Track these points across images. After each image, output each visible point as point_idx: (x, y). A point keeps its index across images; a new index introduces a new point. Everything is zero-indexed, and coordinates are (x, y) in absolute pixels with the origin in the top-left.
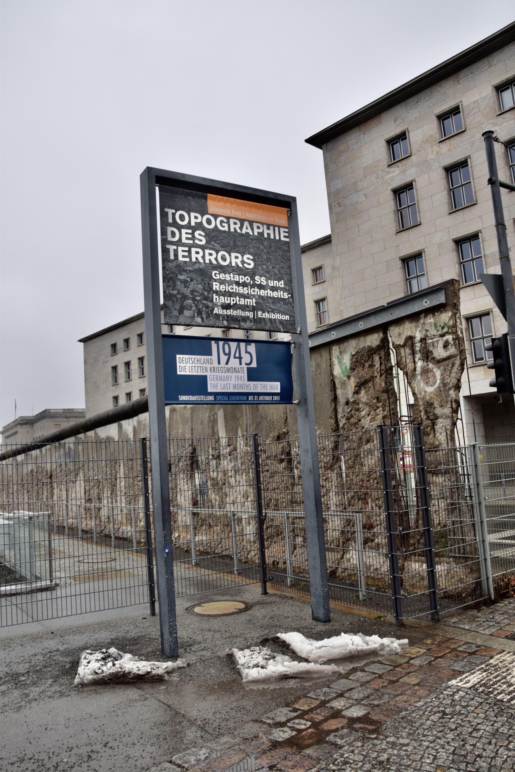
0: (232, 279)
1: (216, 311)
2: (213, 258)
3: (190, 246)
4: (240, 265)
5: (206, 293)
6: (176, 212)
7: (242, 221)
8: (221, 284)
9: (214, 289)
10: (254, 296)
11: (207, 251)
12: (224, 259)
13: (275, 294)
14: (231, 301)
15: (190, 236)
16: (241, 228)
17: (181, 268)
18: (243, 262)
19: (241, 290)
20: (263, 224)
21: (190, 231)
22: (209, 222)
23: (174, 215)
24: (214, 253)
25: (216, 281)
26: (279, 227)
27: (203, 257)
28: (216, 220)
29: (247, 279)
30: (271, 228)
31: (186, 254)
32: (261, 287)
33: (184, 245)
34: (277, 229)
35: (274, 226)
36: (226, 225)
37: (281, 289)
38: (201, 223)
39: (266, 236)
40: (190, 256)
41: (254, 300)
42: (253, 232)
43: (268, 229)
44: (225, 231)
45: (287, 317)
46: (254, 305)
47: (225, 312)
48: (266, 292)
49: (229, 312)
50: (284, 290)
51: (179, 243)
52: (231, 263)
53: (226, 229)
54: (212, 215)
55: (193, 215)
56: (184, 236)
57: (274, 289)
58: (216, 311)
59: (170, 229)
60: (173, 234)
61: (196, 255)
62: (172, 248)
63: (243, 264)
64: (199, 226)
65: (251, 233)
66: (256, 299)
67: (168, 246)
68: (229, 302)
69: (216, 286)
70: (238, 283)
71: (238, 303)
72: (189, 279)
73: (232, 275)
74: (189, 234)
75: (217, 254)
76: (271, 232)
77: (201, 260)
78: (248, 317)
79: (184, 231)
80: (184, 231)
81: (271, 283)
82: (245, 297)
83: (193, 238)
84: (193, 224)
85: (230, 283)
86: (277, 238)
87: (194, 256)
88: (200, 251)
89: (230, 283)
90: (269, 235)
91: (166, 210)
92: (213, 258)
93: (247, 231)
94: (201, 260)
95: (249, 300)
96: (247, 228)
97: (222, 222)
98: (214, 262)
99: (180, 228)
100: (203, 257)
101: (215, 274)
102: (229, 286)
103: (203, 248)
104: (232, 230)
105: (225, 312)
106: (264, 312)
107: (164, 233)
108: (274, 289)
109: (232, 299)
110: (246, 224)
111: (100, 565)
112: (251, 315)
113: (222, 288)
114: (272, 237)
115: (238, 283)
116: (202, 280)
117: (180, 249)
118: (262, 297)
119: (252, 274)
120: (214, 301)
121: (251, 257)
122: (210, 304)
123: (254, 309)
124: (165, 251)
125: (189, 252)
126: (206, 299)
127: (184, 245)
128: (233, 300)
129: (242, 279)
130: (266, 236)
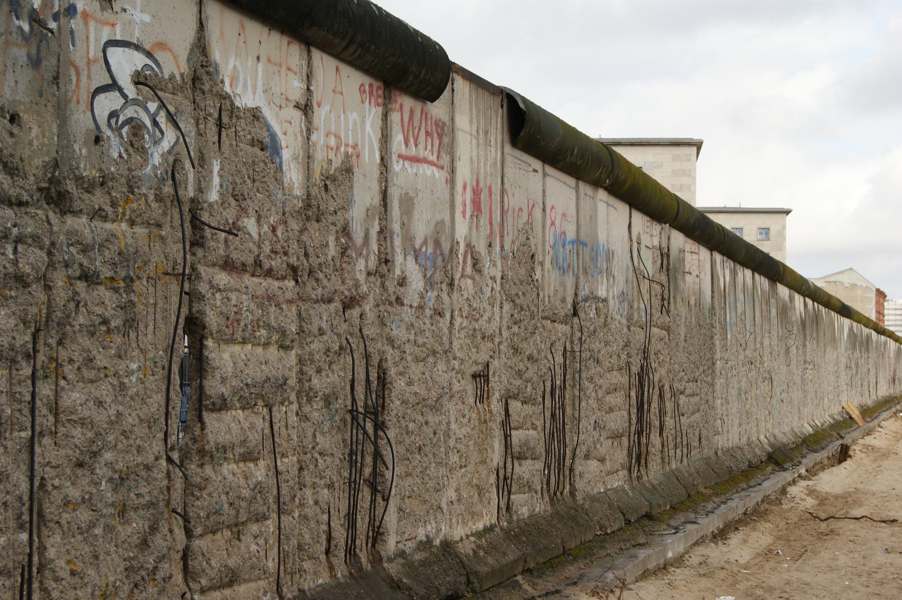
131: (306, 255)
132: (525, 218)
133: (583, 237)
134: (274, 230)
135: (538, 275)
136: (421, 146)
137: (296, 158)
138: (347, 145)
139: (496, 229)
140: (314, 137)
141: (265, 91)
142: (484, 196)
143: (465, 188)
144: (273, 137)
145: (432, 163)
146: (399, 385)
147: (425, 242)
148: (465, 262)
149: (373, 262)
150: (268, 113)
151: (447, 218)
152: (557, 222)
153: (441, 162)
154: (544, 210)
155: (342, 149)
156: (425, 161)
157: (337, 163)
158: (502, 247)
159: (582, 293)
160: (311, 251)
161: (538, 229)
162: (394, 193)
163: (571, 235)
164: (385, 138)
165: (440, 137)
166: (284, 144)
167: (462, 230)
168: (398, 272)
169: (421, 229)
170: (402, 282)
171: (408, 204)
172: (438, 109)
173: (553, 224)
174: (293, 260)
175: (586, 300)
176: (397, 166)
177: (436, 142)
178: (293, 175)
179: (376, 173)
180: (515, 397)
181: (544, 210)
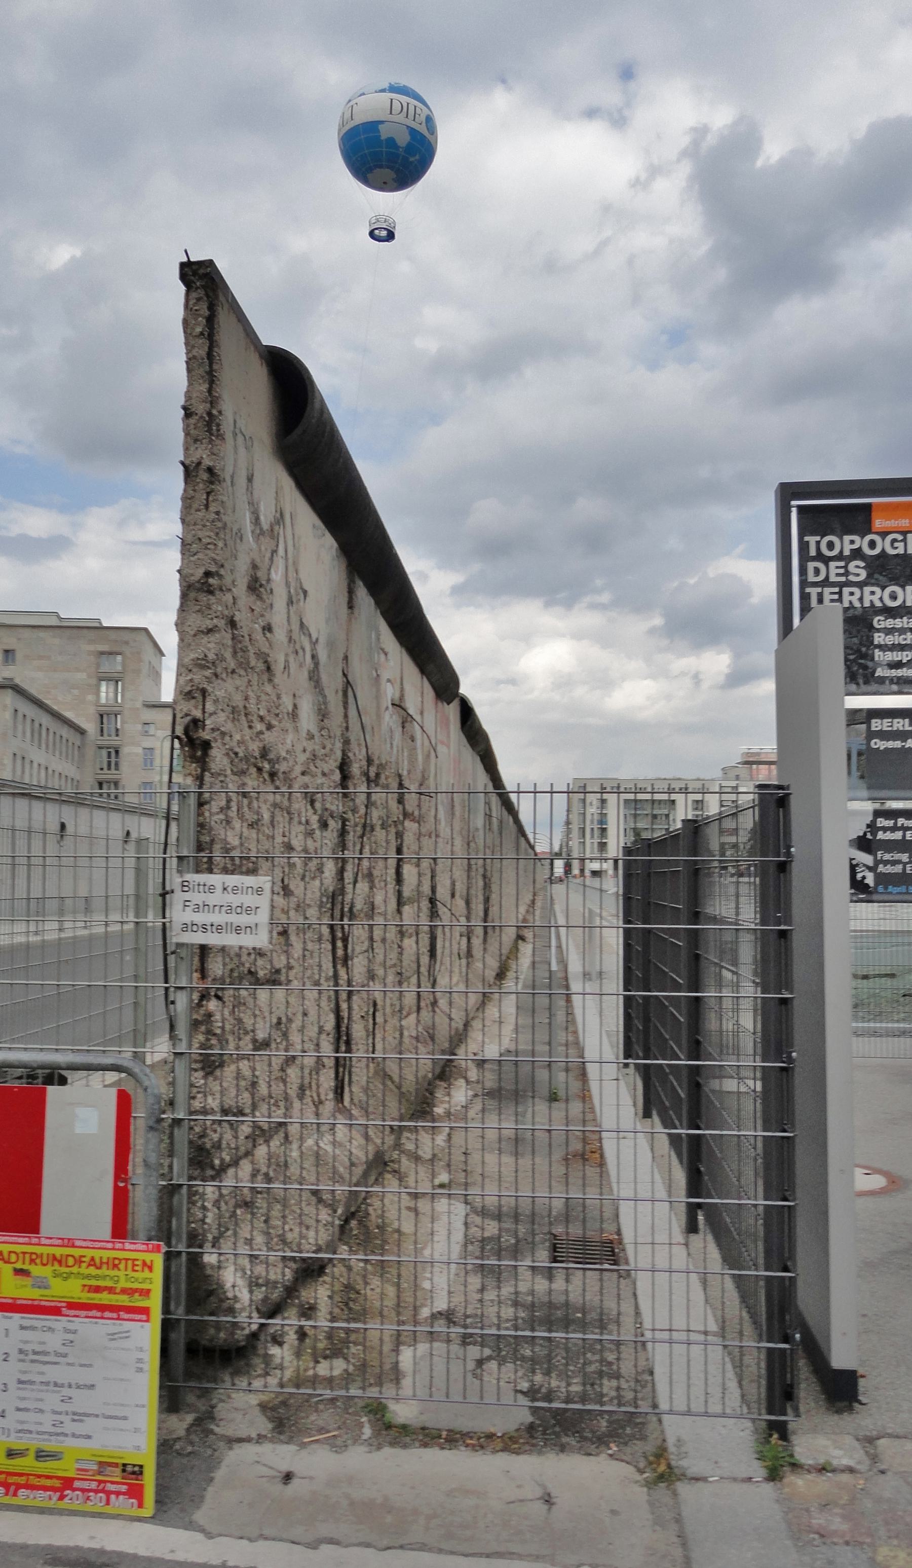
1: (879, 672)
3: (841, 585)
5: (864, 649)
8: (887, 635)
11: (867, 590)
12: (894, 597)
21: (842, 564)
22: (872, 544)
23: (818, 543)
24: (877, 590)
25: (878, 630)
27: (861, 599)
31: (836, 597)
33: (833, 585)
47: (894, 673)
49: (900, 672)
51: (826, 583)
53: (901, 551)
54: (877, 533)
55: (847, 538)
56: (833, 571)
58: (879, 672)
59: (811, 565)
60: (817, 571)
64: (857, 554)
67: (808, 590)
69: (878, 638)
77: (857, 604)
80: (833, 564)
83: (847, 573)
87: (846, 598)
88: (856, 590)
91: (806, 539)
97: (894, 541)
99: (826, 560)
100: (861, 599)
103: (861, 585)
105: (894, 673)
107: (803, 571)
113: (889, 640)
116: (859, 631)
117: (827, 591)
122: (870, 664)
125: (840, 593)
126: (864, 656)
127: (833, 585)
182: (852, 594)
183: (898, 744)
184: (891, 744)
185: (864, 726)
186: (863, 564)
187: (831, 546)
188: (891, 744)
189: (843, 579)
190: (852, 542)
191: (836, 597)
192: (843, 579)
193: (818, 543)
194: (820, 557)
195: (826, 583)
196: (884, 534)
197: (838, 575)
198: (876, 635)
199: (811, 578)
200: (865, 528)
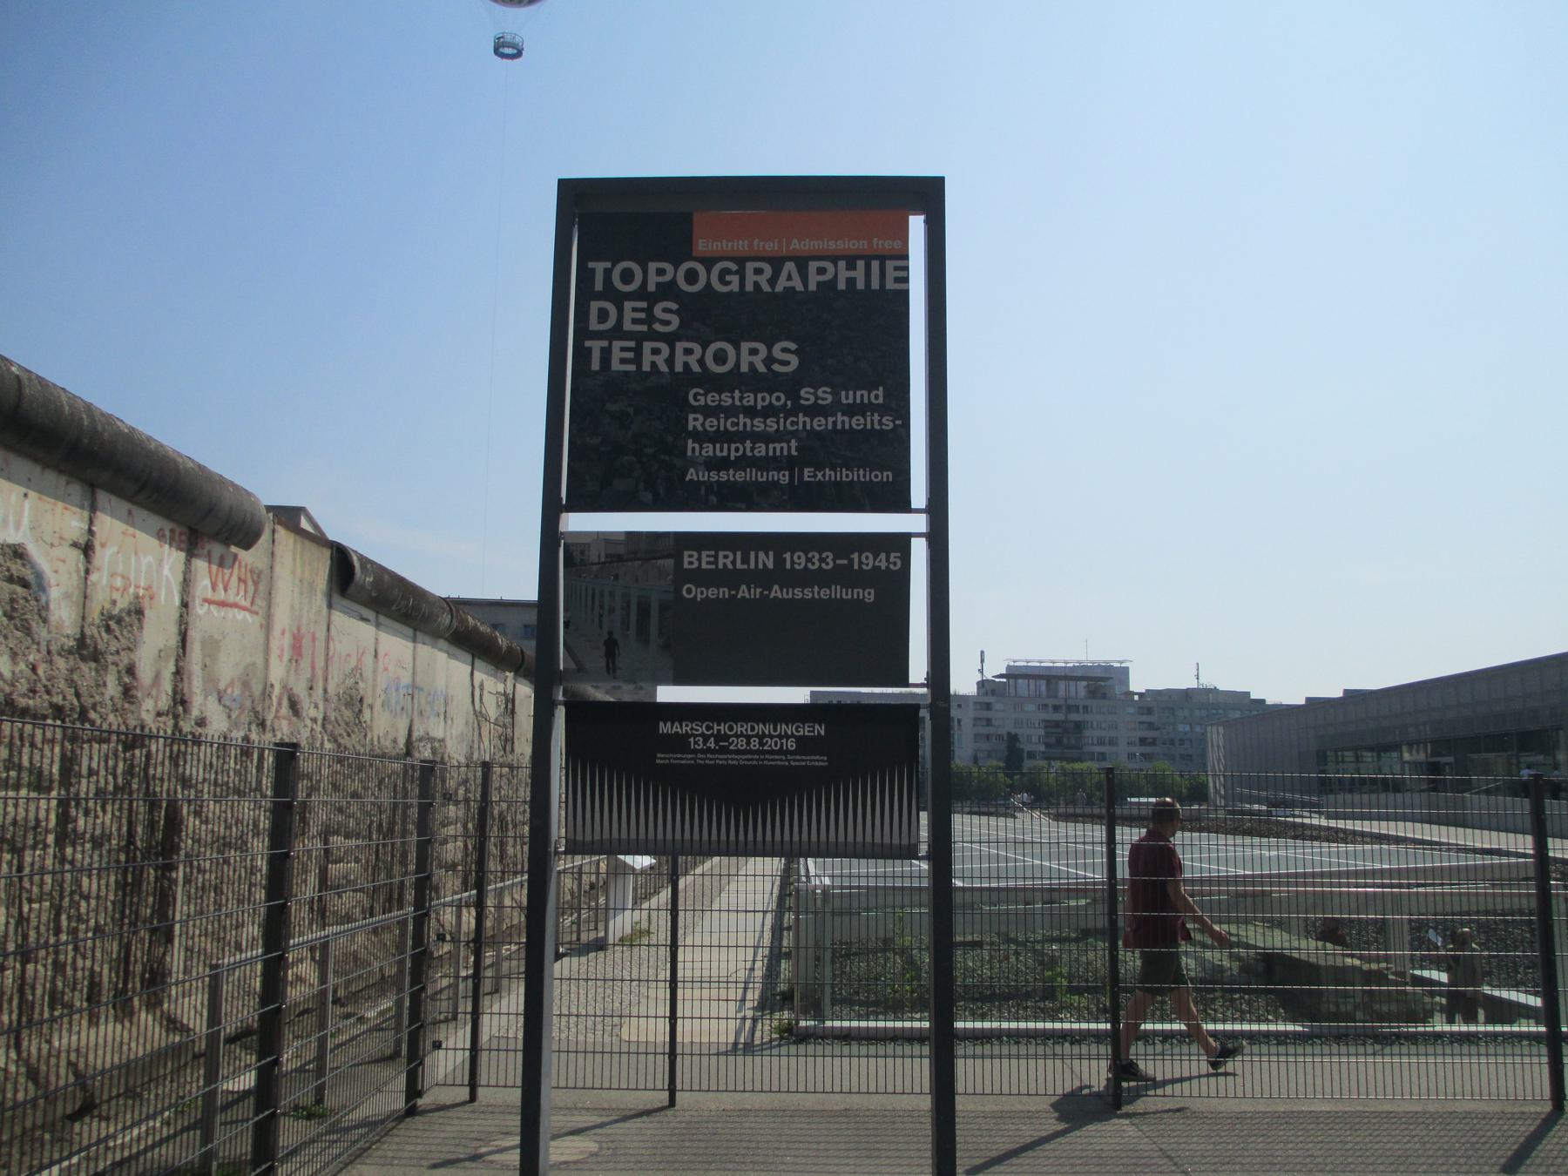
0: (738, 403)
1: (691, 475)
2: (692, 361)
3: (640, 338)
4: (762, 369)
5: (670, 439)
6: (614, 266)
7: (777, 263)
9: (690, 428)
10: (794, 434)
12: (720, 358)
13: (857, 423)
14: (733, 451)
15: (642, 315)
16: (773, 281)
17: (615, 386)
18: (770, 360)
19: (759, 425)
20: (834, 260)
21: (644, 305)
22: (692, 277)
23: (608, 272)
25: (695, 410)
26: (883, 259)
27: (670, 361)
28: (709, 272)
29: (778, 399)
30: (861, 264)
31: (630, 355)
32: (815, 411)
34: (875, 265)
35: (868, 260)
36: (735, 279)
37: (873, 408)
38: (673, 281)
39: (842, 286)
40: (638, 360)
41: (793, 443)
42: (805, 284)
43: (851, 266)
44: (730, 293)
45: (888, 476)
46: (794, 453)
47: (714, 477)
48: (831, 420)
50: (883, 410)
51: (618, 332)
52: (738, 365)
53: (735, 287)
54: (701, 260)
55: (653, 266)
56: (629, 315)
57: (851, 410)
58: (691, 475)
59: (595, 306)
61: (654, 357)
62: (596, 346)
63: (768, 367)
64: (668, 290)
65: (800, 288)
66: (799, 440)
67: (588, 344)
68: (725, 453)
69: (694, 422)
70: (751, 412)
71: (749, 453)
72: (631, 410)
73: (737, 394)
74: (641, 310)
75: (704, 349)
76: (859, 274)
77: (664, 368)
78: (775, 484)
79: (628, 305)
80: (628, 305)
81: (847, 398)
82: (766, 438)
83: (650, 319)
84: (651, 288)
85: (731, 412)
86: (875, 285)
87: (647, 359)
89: (731, 412)
90: (851, 282)
91: (591, 265)
92: (692, 361)
93: (789, 284)
94: (664, 368)
95: (778, 446)
96: (789, 278)
98: (696, 368)
99: (619, 299)
100: (670, 361)
101: (695, 395)
102: (726, 419)
103: (671, 339)
104: (749, 288)
106: (819, 467)
108: (851, 410)
109: (733, 446)
110: (790, 266)
111: (643, 1012)
112: (784, 477)
113: (711, 424)
114: (860, 285)
115: (751, 412)
117: (617, 345)
118: (819, 433)
119: (791, 385)
120: (689, 453)
121: (793, 346)
123: (790, 463)
124: (582, 354)
125: (638, 351)
128: (737, 450)
129: (763, 400)
130: (842, 286)
131: (78, 695)
132: (353, 663)
133: (419, 682)
134: (34, 669)
135: (367, 715)
136: (232, 592)
137: (67, 596)
138: (137, 587)
139: (319, 673)
140: (93, 577)
141: (33, 528)
142: (306, 642)
143: (283, 633)
144: (39, 576)
145: (244, 609)
146: (192, 823)
147: (231, 684)
148: (280, 704)
149: (164, 703)
150: (33, 550)
151: (260, 661)
152: (391, 668)
153: (255, 608)
154: (376, 656)
155: (131, 590)
156: (235, 605)
157: (123, 603)
158: (325, 690)
159: (415, 735)
160: (83, 691)
161: (368, 673)
162: (195, 636)
163: (406, 679)
164: (187, 583)
165: (256, 583)
166: (53, 582)
167: (277, 673)
168: (195, 712)
169: (228, 669)
170: (201, 722)
171: (212, 646)
172: (250, 558)
173: (386, 669)
174: (58, 699)
175: (421, 740)
176: (199, 609)
177: (251, 588)
178: (63, 616)
179: (175, 615)
180: (337, 832)
181: (376, 656)
182: (656, 352)
183: (724, 592)
184: (712, 593)
185: (670, 562)
186: (674, 306)
187: (627, 276)
188: (712, 593)
189: (644, 328)
190: (661, 272)
191: (630, 355)
192: (644, 328)
193: (608, 272)
194: (610, 293)
195: (618, 332)
196: (709, 263)
197: (635, 321)
198: (691, 416)
199: (594, 325)
200: (679, 250)
